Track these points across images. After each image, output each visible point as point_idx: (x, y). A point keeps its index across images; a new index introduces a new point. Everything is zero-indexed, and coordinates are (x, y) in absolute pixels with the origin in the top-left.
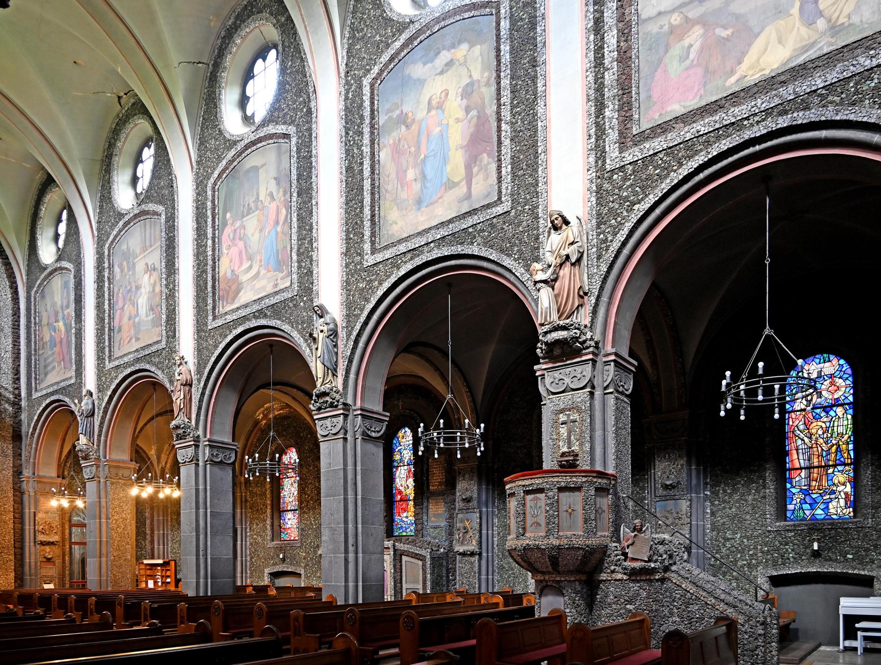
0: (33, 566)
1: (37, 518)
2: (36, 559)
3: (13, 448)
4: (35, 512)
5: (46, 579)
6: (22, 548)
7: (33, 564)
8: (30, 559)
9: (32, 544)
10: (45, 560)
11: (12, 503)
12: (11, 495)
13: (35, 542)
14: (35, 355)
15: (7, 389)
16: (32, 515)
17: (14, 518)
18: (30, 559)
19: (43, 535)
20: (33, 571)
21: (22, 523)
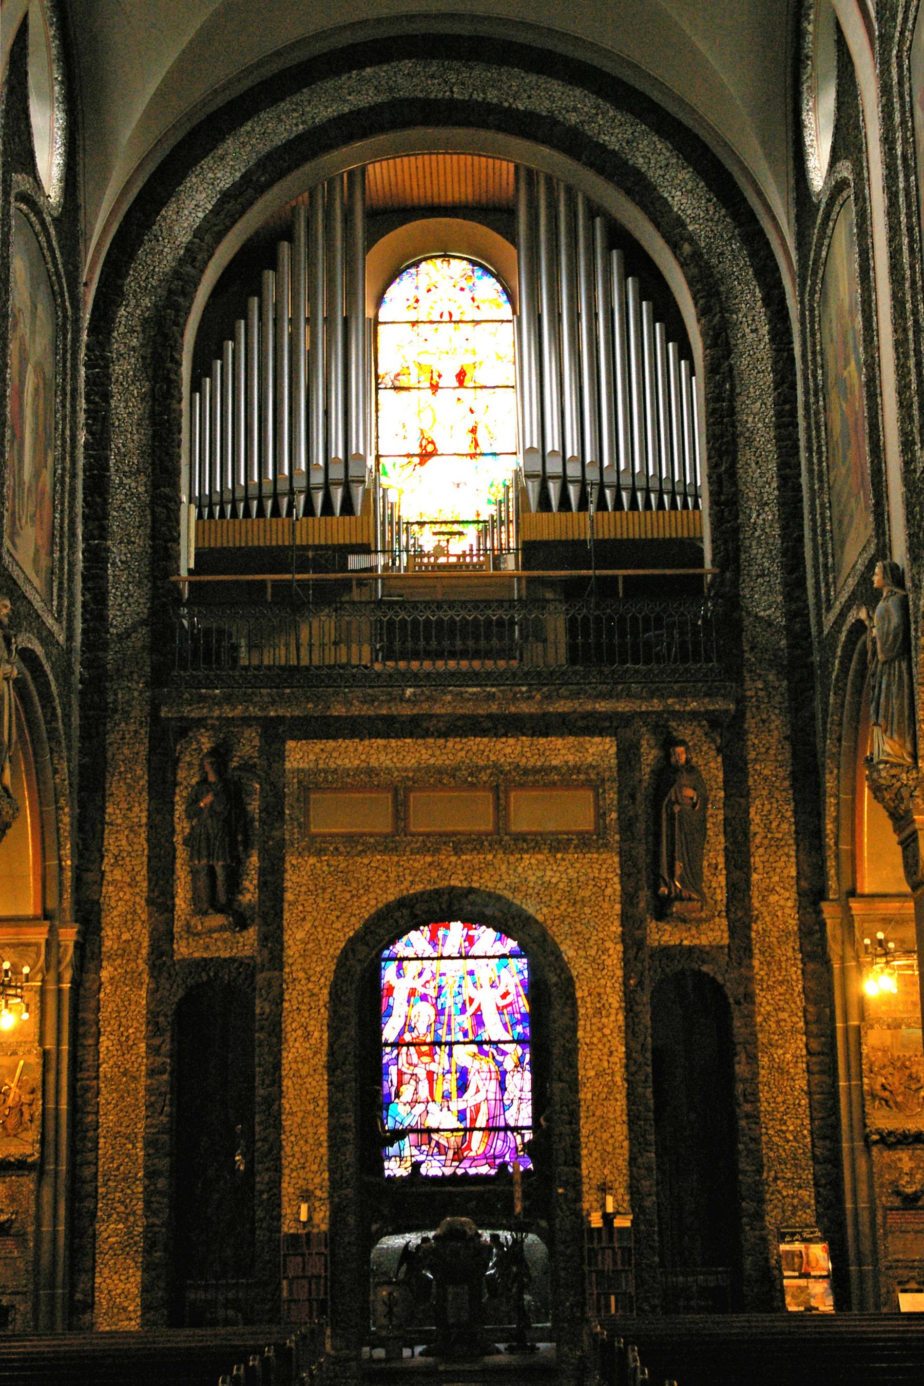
0: (865, 1229)
1: (865, 1050)
2: (872, 1200)
3: (795, 812)
4: (858, 1029)
5: (905, 1273)
6: (835, 1160)
7: (865, 1217)
8: (855, 1202)
9: (859, 1144)
10: (897, 1202)
11: (800, 1001)
12: (795, 973)
13: (866, 1138)
14: (821, 488)
15: (770, 625)
16: (852, 1036)
17: (809, 1053)
18: (855, 1202)
19: (885, 1111)
20: (866, 1245)
21: (832, 1071)
